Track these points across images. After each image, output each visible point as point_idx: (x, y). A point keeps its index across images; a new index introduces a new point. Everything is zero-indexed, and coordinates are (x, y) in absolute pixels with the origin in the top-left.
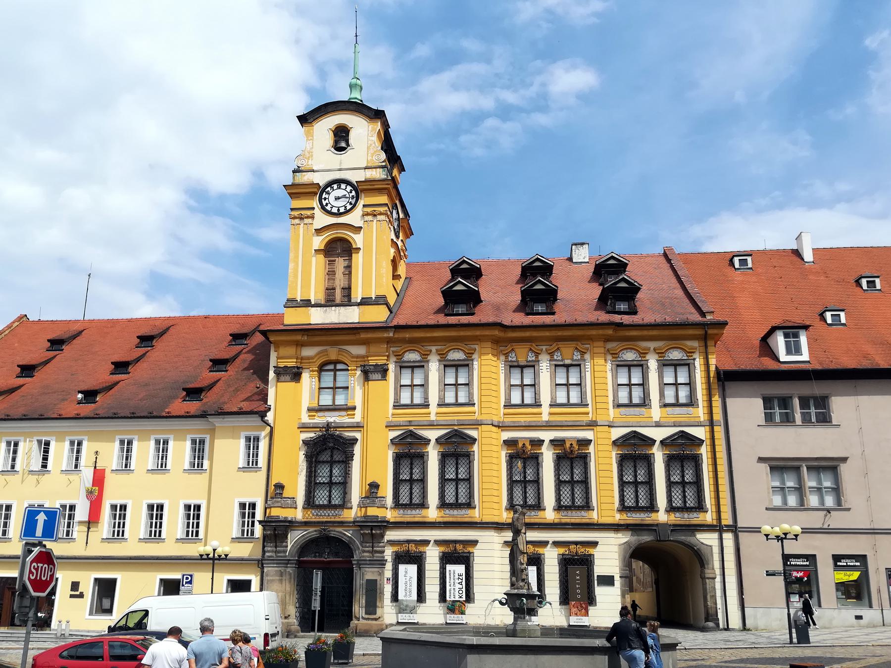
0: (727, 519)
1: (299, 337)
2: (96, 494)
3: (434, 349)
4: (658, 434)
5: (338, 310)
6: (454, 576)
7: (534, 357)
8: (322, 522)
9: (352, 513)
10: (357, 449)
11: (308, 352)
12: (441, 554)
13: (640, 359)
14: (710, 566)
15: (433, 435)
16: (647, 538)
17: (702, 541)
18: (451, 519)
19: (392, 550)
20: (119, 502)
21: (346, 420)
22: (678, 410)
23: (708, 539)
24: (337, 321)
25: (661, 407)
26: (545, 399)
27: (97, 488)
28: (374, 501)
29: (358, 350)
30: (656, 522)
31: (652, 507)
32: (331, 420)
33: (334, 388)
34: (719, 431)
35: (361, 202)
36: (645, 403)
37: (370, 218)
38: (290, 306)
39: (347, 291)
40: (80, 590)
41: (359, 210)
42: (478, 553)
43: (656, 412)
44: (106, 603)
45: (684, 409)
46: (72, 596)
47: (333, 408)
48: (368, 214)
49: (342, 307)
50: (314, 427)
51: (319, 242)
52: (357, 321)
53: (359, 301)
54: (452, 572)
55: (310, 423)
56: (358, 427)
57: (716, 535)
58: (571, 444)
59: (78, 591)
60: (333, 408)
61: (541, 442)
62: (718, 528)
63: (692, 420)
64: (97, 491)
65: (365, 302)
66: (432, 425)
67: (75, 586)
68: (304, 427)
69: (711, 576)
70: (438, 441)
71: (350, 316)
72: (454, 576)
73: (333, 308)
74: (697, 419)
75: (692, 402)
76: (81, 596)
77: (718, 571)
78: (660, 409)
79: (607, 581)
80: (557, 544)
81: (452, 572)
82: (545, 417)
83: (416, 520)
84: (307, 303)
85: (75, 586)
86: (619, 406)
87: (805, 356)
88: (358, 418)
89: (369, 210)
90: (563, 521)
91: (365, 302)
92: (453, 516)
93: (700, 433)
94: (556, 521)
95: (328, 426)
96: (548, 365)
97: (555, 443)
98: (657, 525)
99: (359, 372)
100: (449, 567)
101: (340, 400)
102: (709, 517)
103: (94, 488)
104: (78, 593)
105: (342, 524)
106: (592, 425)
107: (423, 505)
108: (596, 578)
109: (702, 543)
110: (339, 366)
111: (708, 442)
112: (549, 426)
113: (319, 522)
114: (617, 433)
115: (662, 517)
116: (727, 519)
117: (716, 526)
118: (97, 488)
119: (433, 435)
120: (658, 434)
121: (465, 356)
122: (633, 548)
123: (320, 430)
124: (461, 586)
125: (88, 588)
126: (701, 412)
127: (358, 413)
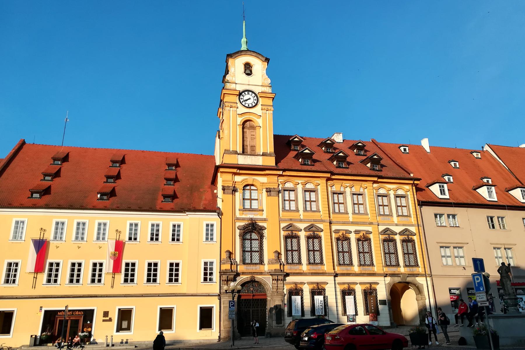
0: (428, 272)
1: (235, 170)
2: (117, 256)
3: (300, 182)
4: (398, 229)
5: (251, 158)
6: (318, 302)
7: (343, 189)
8: (252, 273)
9: (266, 268)
10: (265, 233)
11: (238, 178)
12: (310, 290)
13: (387, 193)
14: (423, 294)
15: (302, 226)
16: (397, 279)
17: (419, 282)
18: (314, 271)
19: (286, 288)
20: (130, 261)
21: (258, 217)
22: (404, 218)
23: (421, 280)
24: (251, 164)
25: (397, 217)
26: (350, 210)
27: (117, 252)
28: (278, 261)
29: (263, 179)
30: (400, 273)
31: (398, 265)
32: (251, 216)
33: (251, 199)
34: (421, 229)
35: (260, 102)
36: (391, 215)
37: (265, 111)
38: (227, 153)
39: (253, 147)
40: (110, 316)
41: (259, 107)
42: (327, 287)
43: (395, 219)
44: (125, 324)
45: (406, 218)
46: (104, 321)
47: (251, 210)
48: (264, 109)
49: (253, 156)
50: (243, 219)
51: (240, 120)
52: (261, 164)
53: (261, 154)
54: (317, 299)
55: (241, 218)
56: (265, 220)
57: (424, 278)
58: (363, 234)
59: (108, 317)
60: (251, 210)
61: (351, 232)
62: (425, 275)
63: (410, 223)
64: (117, 254)
65: (264, 155)
66: (301, 221)
67: (106, 314)
68: (238, 219)
69: (424, 299)
70: (305, 229)
71: (259, 161)
72: (318, 302)
73: (249, 156)
74: (411, 223)
75: (409, 216)
76: (110, 320)
77: (427, 297)
78: (396, 218)
79: (383, 302)
80: (361, 283)
81: (317, 299)
82: (351, 219)
83: (297, 271)
84: (236, 153)
85: (106, 314)
86: (380, 215)
87: (447, 196)
88: (264, 216)
89: (264, 107)
90: (362, 272)
91: (264, 155)
92: (314, 270)
93: (413, 229)
94: (359, 272)
95: (251, 219)
96: (350, 194)
97: (357, 232)
98: (401, 274)
99: (264, 190)
100: (316, 297)
101: (255, 205)
102: (421, 270)
103: (116, 252)
104: (108, 318)
105: (261, 273)
106: (371, 224)
107: (300, 263)
108: (378, 301)
109: (419, 283)
110: (252, 188)
111: (418, 234)
112: (353, 223)
113: (250, 273)
114: (382, 228)
115: (402, 270)
116: (428, 272)
117: (424, 274)
118: (117, 252)
119: (302, 226)
120: (398, 229)
121: (314, 187)
122: (392, 286)
123: (248, 222)
124: (322, 307)
125: (115, 316)
126: (413, 220)
127: (265, 212)
